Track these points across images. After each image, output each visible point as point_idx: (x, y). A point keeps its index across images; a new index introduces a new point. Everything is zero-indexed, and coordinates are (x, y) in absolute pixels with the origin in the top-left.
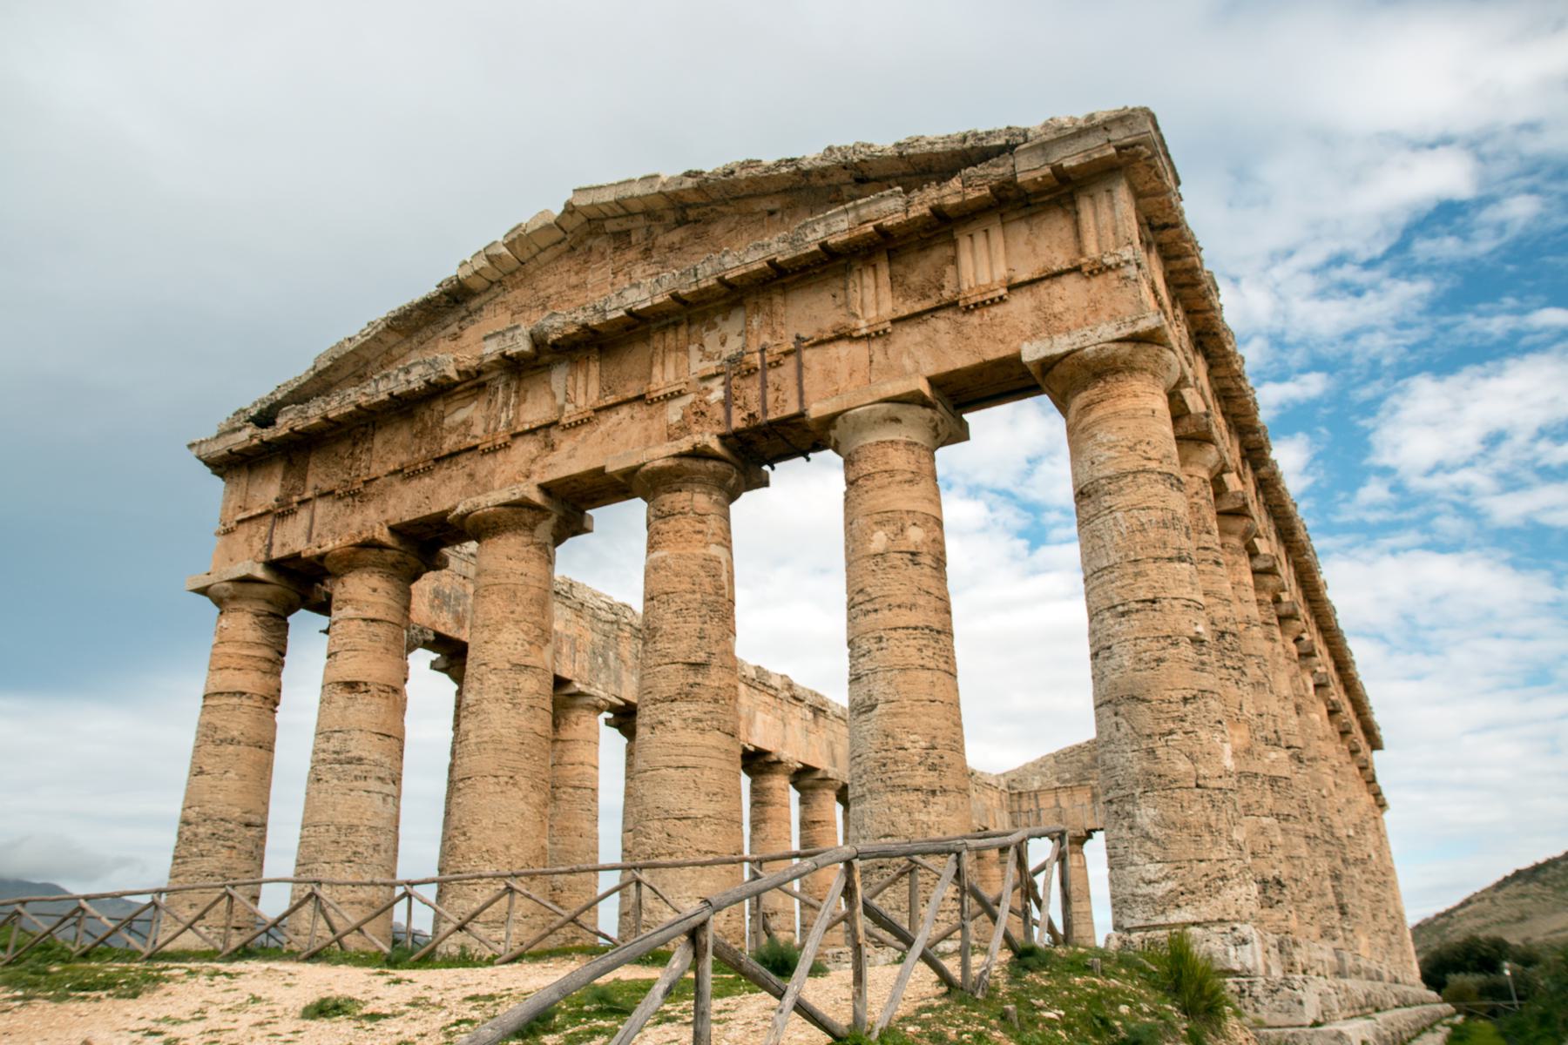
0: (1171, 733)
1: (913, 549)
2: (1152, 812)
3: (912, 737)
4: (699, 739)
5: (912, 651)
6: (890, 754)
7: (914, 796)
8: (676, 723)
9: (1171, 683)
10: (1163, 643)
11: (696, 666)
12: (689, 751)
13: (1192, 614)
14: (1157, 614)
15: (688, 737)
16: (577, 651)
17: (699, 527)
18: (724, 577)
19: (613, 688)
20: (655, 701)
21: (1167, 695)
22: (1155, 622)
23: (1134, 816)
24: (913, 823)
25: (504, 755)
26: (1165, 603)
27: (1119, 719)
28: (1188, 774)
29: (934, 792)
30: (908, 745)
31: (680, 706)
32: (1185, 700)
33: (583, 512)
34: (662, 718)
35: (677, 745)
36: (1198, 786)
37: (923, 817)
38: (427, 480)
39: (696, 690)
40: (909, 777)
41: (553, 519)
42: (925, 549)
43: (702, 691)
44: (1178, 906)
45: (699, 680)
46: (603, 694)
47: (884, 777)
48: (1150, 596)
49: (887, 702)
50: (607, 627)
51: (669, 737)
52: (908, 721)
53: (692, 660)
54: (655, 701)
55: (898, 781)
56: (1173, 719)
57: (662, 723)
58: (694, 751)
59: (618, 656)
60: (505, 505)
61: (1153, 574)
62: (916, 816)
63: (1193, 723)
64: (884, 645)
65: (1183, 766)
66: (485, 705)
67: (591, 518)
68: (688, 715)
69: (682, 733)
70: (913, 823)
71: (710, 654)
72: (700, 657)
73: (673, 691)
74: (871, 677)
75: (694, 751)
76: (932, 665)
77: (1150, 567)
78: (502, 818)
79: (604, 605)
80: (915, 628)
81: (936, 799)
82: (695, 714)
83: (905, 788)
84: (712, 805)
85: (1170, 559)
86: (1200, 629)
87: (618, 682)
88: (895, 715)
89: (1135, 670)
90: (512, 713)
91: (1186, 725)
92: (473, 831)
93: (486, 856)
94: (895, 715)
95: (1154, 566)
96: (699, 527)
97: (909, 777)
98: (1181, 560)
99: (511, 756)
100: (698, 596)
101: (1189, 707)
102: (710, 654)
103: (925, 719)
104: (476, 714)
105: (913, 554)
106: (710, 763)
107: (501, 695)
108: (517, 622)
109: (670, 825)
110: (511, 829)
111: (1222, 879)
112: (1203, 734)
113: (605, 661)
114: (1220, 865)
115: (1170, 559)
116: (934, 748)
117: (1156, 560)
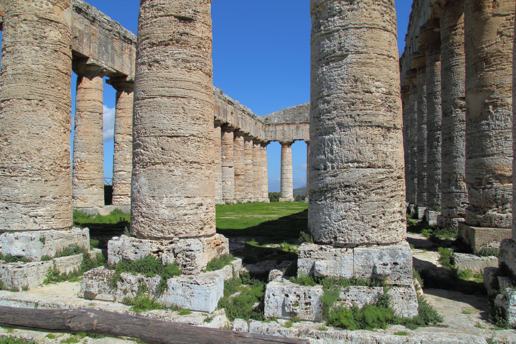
3: (377, 83)
4: (187, 76)
5: (376, 14)
6: (359, 96)
7: (376, 131)
8: (170, 62)
12: (179, 84)
15: (176, 73)
16: (91, 42)
19: (110, 64)
20: (153, 44)
24: (375, 152)
25: (34, 84)
29: (388, 129)
30: (373, 89)
31: (171, 49)
34: (157, 57)
35: (171, 79)
37: (383, 148)
39: (184, 38)
40: (374, 115)
43: (190, 39)
45: (188, 30)
46: (105, 66)
47: (354, 114)
49: (357, 53)
50: (107, 32)
51: (163, 73)
52: (373, 70)
53: (183, 14)
54: (153, 44)
57: (157, 62)
58: (183, 84)
59: (113, 48)
62: (378, 147)
66: (18, 47)
68: (180, 56)
69: (173, 70)
71: (196, 12)
72: (188, 13)
73: (167, 37)
74: (342, 33)
75: (183, 84)
78: (34, 130)
79: (105, 21)
81: (391, 134)
82: (185, 56)
83: (370, 125)
84: (196, 127)
87: (113, 61)
88: (364, 64)
90: (40, 53)
92: (13, 138)
93: (24, 156)
94: (364, 64)
97: (374, 115)
99: (40, 85)
103: (385, 70)
104: (11, 53)
106: (194, 95)
107: (31, 39)
109: (163, 141)
110: (42, 138)
113: (106, 50)
116: (391, 94)
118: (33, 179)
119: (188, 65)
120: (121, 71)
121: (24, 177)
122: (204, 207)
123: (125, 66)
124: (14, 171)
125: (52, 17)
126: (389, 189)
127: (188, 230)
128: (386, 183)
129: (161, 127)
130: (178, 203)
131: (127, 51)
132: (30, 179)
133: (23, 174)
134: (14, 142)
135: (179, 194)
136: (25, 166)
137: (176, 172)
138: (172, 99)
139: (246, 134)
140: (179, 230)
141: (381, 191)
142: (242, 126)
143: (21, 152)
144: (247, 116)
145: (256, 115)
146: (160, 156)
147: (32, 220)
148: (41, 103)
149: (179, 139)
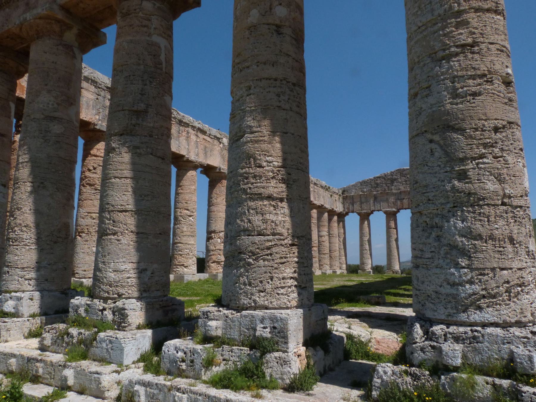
0: (482, 156)
1: (278, 22)
2: (460, 224)
3: (268, 159)
9: (485, 114)
10: (479, 81)
11: (138, 113)
13: (503, 58)
14: (476, 56)
17: (146, 22)
18: (163, 57)
21: (480, 124)
22: (474, 64)
23: (441, 228)
26: (483, 46)
27: (433, 146)
28: (495, 192)
30: (265, 164)
32: (496, 130)
33: (98, 30)
36: (503, 204)
37: (272, 217)
38: (7, 9)
40: (263, 188)
41: (75, 31)
42: (287, 24)
44: (480, 308)
48: (470, 40)
49: (252, 133)
53: (135, 108)
55: (255, 191)
56: (485, 146)
60: (40, 18)
61: (474, 22)
62: (267, 216)
63: (502, 150)
64: (252, 91)
65: (491, 186)
67: (105, 34)
70: (265, 221)
72: (142, 106)
76: (287, 107)
77: (472, 17)
80: (276, 80)
85: (488, 10)
86: (510, 71)
89: (451, 103)
91: (496, 150)
93: (24, 229)
94: (257, 142)
95: (472, 15)
96: (146, 22)
98: (497, 12)
100: (142, 67)
101: (499, 135)
102: (148, 106)
105: (278, 26)
108: (49, 91)
111: (520, 286)
112: (510, 159)
114: (519, 273)
115: (488, 10)
117: (477, 10)
118: (31, 247)
119: (138, 151)
120: (178, 152)
121: (24, 246)
122: (149, 273)
123: (182, 147)
124: (16, 241)
125: (56, 114)
126: (278, 256)
127: (130, 292)
128: (274, 250)
129: (113, 203)
130: (123, 268)
131: (184, 134)
132: (28, 248)
133: (23, 243)
134: (18, 217)
135: (124, 259)
136: (25, 237)
137: (123, 241)
138: (123, 179)
139: (319, 206)
140: (121, 291)
141: (269, 257)
142: (315, 198)
143: (23, 225)
144: (320, 189)
145: (331, 187)
146: (111, 227)
147: (27, 282)
148: (42, 185)
149: (127, 213)
